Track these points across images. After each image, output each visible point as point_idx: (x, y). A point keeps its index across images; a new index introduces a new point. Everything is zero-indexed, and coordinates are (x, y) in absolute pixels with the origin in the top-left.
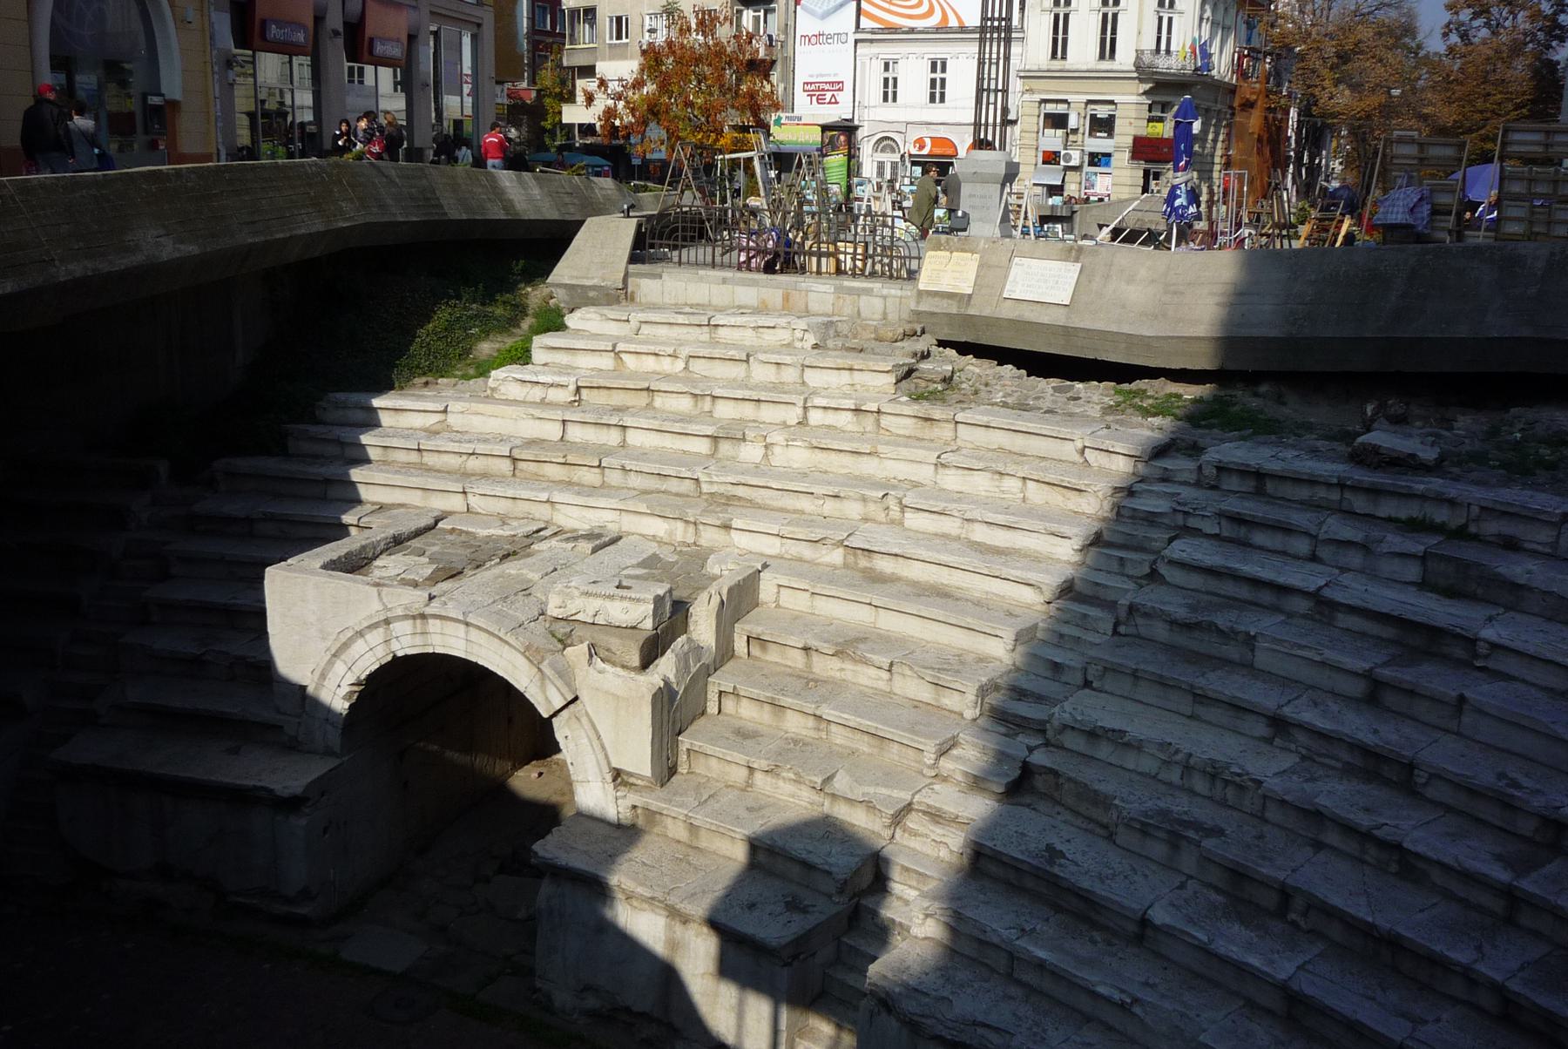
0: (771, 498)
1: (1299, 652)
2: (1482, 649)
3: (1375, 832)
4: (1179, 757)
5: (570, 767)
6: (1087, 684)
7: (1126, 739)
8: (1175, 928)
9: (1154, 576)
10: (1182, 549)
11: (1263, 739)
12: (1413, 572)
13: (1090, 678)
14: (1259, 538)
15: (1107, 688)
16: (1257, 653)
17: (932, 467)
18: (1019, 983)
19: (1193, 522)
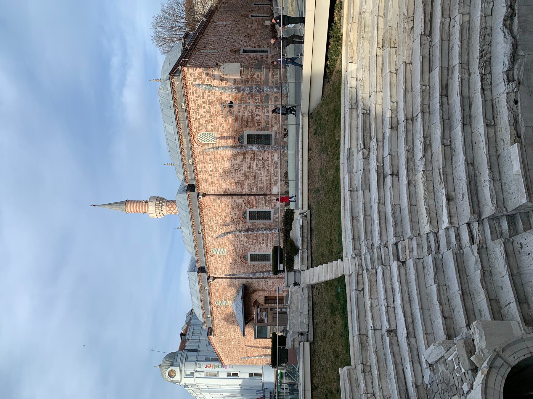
0: (402, 382)
1: (392, 194)
2: (379, 164)
3: (423, 142)
4: (427, 194)
5: (526, 356)
6: (419, 234)
7: (428, 208)
8: (463, 153)
9: (386, 246)
10: (377, 242)
11: (415, 186)
12: (367, 192)
13: (417, 235)
14: (369, 229)
15: (418, 229)
16: (396, 204)
17: (376, 331)
18: (500, 177)
19: (370, 247)
